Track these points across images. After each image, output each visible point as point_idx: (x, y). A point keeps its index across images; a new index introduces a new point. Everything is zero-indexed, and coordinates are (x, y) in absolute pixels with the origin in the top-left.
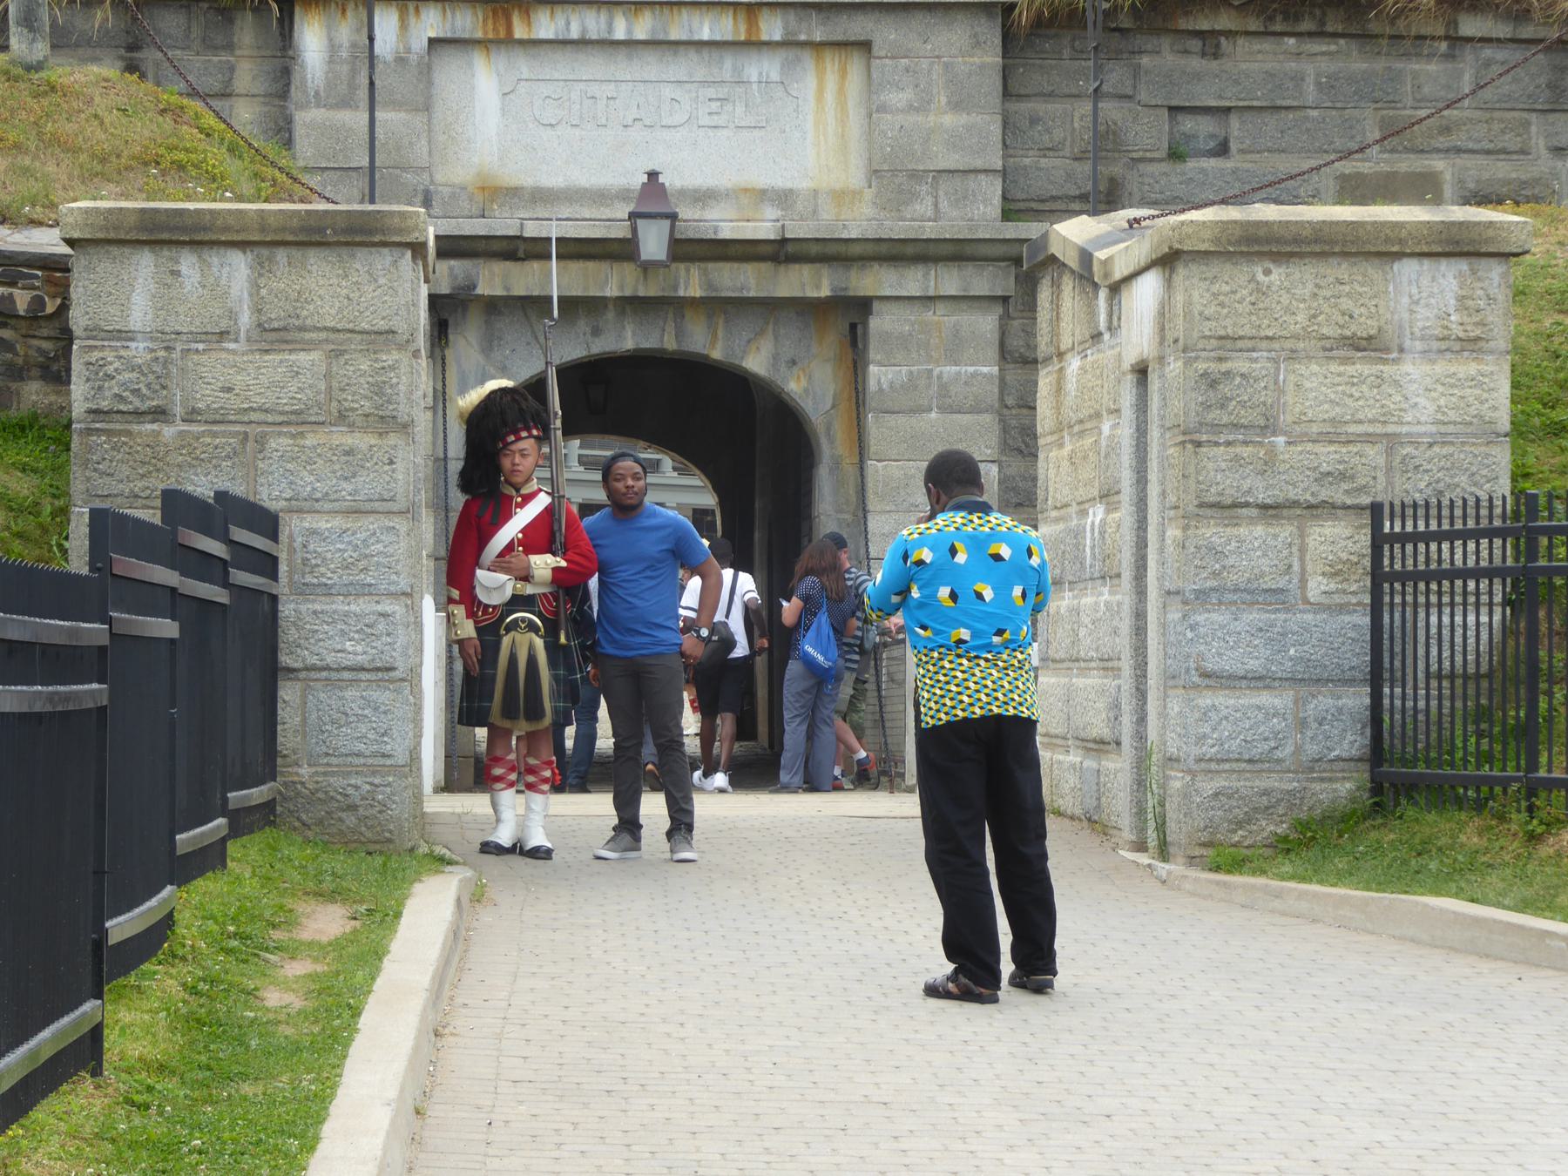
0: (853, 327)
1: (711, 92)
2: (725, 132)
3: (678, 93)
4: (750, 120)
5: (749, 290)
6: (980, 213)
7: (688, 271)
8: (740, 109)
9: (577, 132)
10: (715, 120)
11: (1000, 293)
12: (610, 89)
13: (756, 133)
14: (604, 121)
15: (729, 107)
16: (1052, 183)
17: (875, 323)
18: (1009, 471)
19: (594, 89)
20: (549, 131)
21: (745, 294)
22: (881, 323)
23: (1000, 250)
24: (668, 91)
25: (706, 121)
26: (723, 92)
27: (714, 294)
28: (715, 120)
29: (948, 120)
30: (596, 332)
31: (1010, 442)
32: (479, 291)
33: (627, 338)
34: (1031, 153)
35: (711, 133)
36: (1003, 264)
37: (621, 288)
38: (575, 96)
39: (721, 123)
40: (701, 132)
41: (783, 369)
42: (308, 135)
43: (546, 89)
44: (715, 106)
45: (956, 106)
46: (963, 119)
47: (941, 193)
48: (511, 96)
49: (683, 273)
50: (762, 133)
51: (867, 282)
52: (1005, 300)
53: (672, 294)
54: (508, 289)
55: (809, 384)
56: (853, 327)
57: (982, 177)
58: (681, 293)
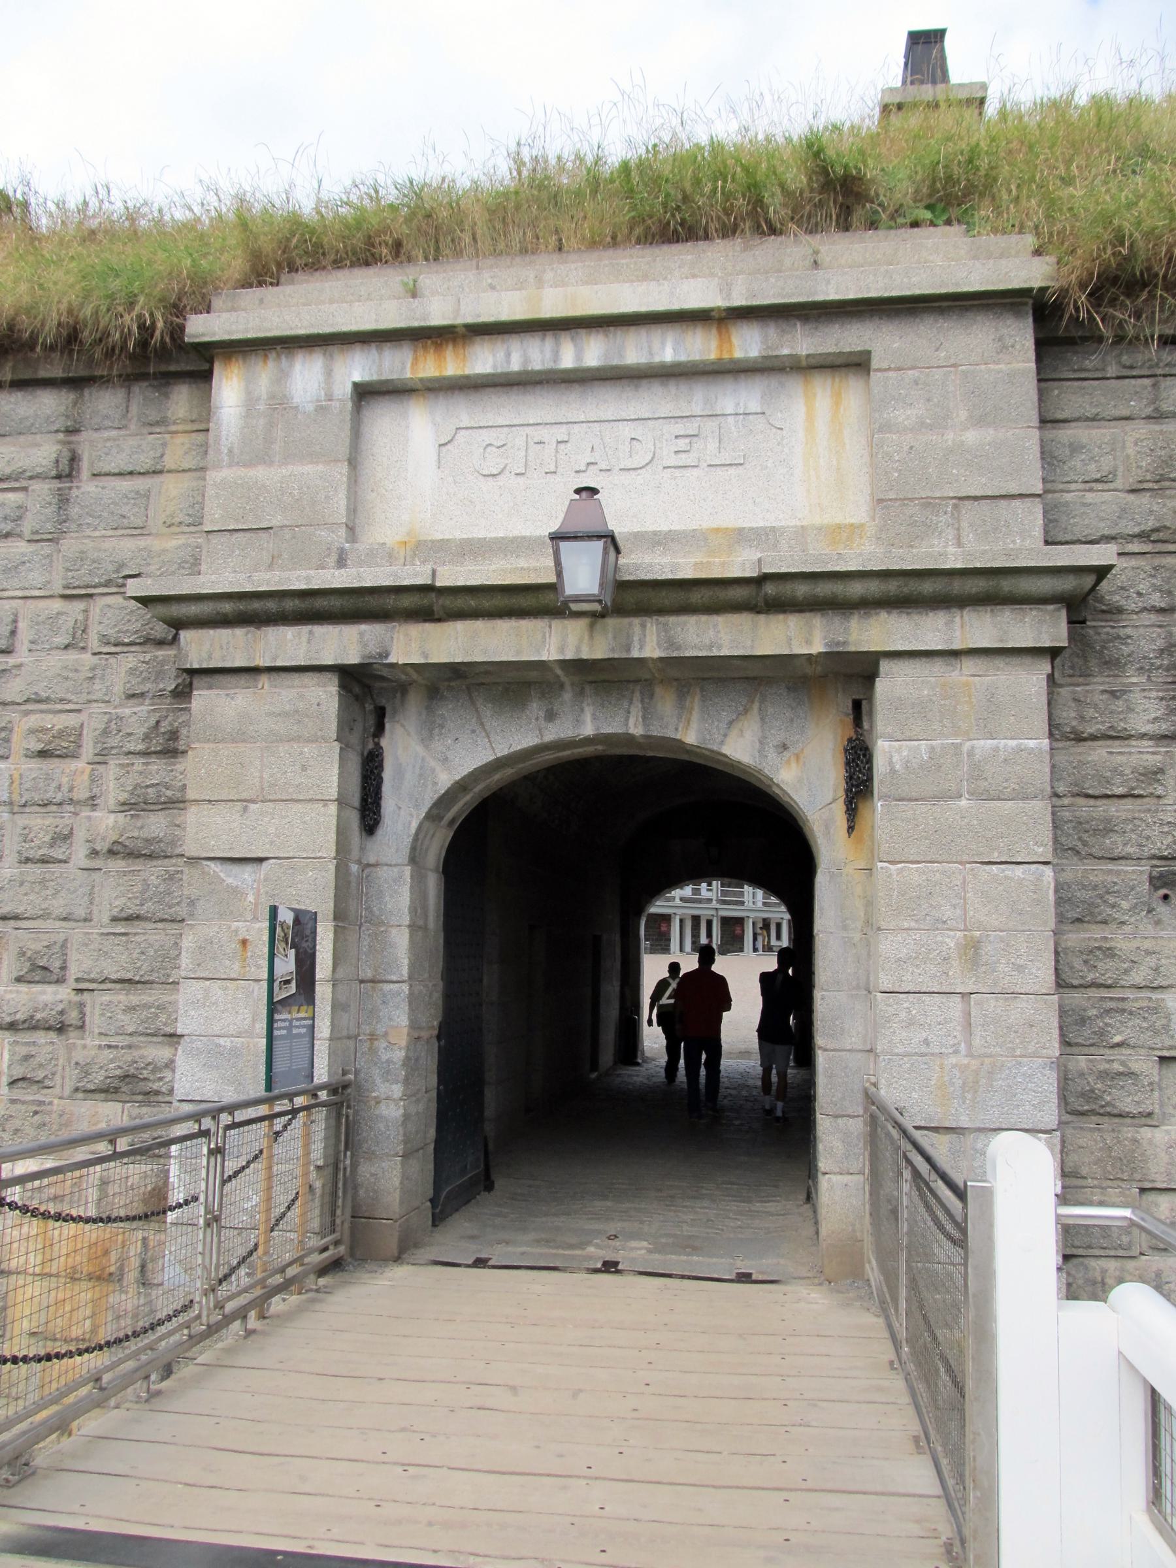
0: (857, 706)
1: (679, 428)
2: (695, 472)
3: (637, 430)
4: (725, 458)
5: (720, 647)
6: (1019, 541)
8: (712, 445)
9: (521, 480)
10: (683, 459)
12: (561, 433)
13: (732, 471)
14: (552, 469)
15: (698, 444)
16: (1102, 519)
17: (881, 686)
18: (1068, 876)
19: (543, 433)
21: (715, 653)
22: (891, 685)
23: (1046, 585)
24: (627, 430)
25: (673, 460)
26: (691, 427)
28: (683, 459)
29: (971, 437)
30: (551, 716)
31: (1063, 839)
32: (392, 659)
33: (585, 723)
34: (1073, 486)
35: (677, 473)
36: (1051, 607)
37: (562, 649)
38: (520, 441)
41: (772, 754)
42: (218, 496)
43: (486, 436)
44: (682, 444)
45: (980, 421)
46: (989, 434)
47: (964, 524)
48: (449, 447)
49: (637, 629)
52: (1053, 653)
53: (624, 655)
54: (426, 657)
55: (800, 768)
56: (857, 706)
57: (1017, 503)
58: (635, 654)
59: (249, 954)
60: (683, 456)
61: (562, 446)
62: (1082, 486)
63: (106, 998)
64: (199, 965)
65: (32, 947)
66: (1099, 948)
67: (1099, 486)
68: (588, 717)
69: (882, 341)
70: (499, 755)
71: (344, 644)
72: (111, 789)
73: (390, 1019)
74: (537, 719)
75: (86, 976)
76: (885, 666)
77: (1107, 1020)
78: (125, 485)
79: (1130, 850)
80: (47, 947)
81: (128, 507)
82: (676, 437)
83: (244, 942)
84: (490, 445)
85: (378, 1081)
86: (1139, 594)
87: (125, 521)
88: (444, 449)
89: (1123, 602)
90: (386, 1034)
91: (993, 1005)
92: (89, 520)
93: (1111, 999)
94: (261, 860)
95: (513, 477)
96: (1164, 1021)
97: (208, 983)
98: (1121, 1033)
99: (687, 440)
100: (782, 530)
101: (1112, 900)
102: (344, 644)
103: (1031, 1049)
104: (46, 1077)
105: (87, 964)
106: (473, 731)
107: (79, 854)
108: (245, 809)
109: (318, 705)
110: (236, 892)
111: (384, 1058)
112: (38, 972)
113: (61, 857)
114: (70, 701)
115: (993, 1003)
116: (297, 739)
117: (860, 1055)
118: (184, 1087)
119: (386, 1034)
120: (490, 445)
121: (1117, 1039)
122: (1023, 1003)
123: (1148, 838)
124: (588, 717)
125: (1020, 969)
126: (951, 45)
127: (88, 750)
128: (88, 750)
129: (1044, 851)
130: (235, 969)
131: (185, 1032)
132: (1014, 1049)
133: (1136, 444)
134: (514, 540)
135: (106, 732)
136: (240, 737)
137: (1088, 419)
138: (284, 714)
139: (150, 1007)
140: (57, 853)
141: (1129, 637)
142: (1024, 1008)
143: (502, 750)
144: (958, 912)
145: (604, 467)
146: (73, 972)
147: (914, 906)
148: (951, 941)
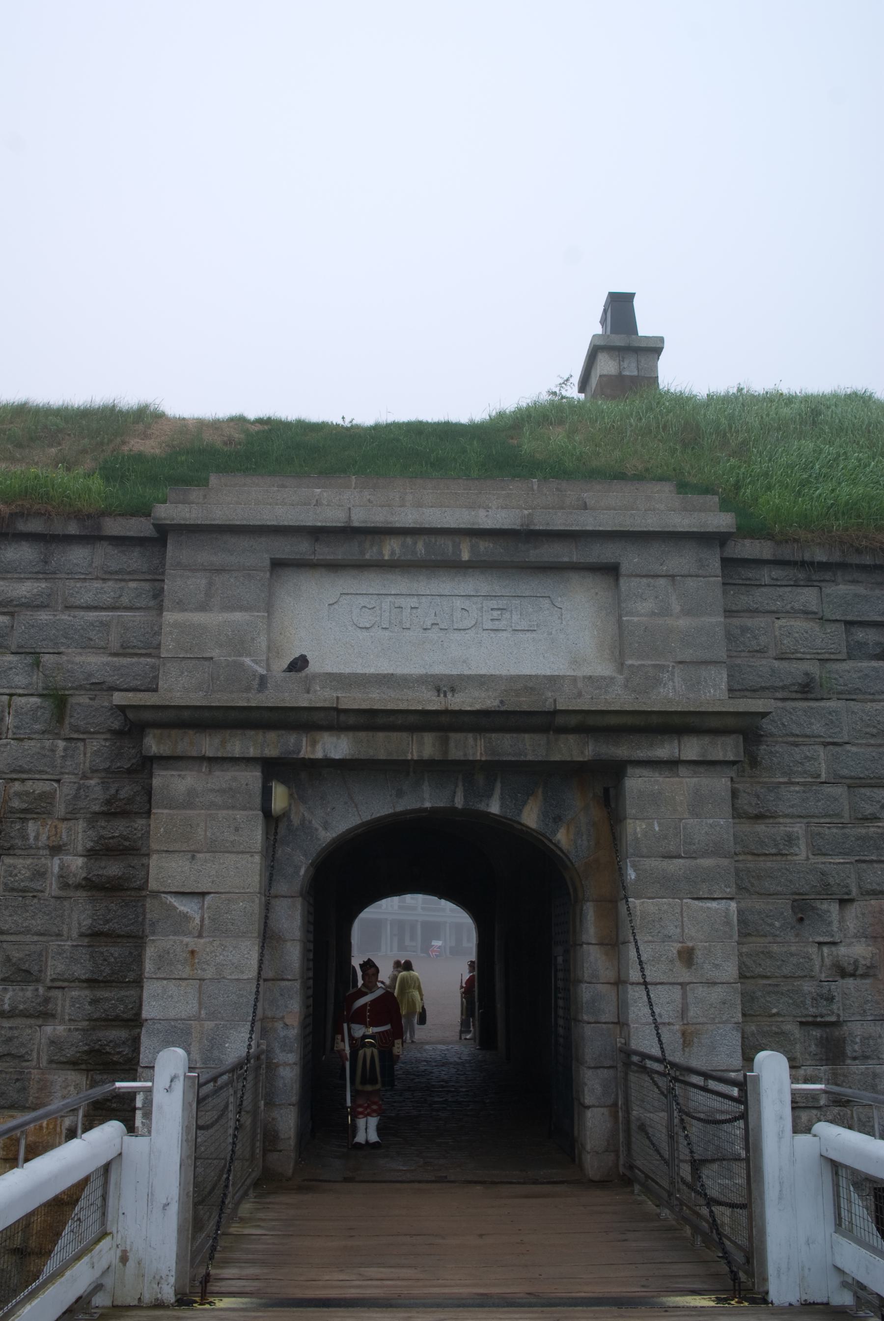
1: (493, 604)
2: (505, 634)
3: (467, 604)
4: (524, 625)
6: (713, 693)
7: (475, 740)
8: (515, 617)
11: (732, 758)
12: (413, 602)
13: (528, 634)
15: (507, 615)
16: (761, 677)
19: (401, 601)
20: (365, 633)
21: (522, 758)
22: (636, 783)
24: (458, 603)
25: (489, 625)
26: (502, 603)
27: (497, 758)
29: (683, 623)
30: (400, 794)
34: (743, 654)
35: (492, 634)
38: (386, 606)
39: (501, 627)
40: (485, 634)
43: (363, 601)
44: (496, 614)
45: (687, 612)
48: (336, 606)
50: (534, 635)
51: (621, 751)
56: (606, 791)
59: (197, 961)
60: (497, 623)
61: (414, 611)
62: (746, 654)
63: (75, 993)
64: (159, 969)
65: (17, 955)
66: (762, 952)
67: (759, 655)
68: (426, 796)
69: (631, 559)
70: (364, 820)
71: (271, 744)
72: (80, 839)
73: (286, 1007)
74: (391, 796)
75: (60, 977)
76: (630, 770)
77: (769, 999)
78: (92, 615)
79: (779, 889)
80: (29, 955)
81: (94, 633)
82: (492, 609)
83: (193, 952)
84: (365, 607)
85: (278, 1051)
86: (783, 724)
87: (92, 643)
88: (332, 608)
89: (773, 730)
90: (283, 1017)
91: (701, 991)
92: (64, 640)
93: (770, 985)
94: (203, 894)
95: (380, 630)
96: (802, 999)
97: (165, 982)
98: (776, 1007)
99: (499, 612)
100: (563, 677)
101: (769, 921)
102: (271, 744)
103: (724, 1018)
104: (27, 1052)
105: (61, 967)
106: (346, 803)
107: (53, 887)
108: (193, 857)
109: (247, 785)
110: (186, 917)
111: (282, 1034)
112: (23, 975)
113: (39, 888)
114: (47, 773)
115: (701, 989)
116: (233, 808)
117: (611, 1026)
118: (147, 1057)
119: (283, 1017)
120: (365, 607)
121: (774, 1011)
122: (719, 989)
123: (791, 881)
124: (426, 796)
125: (717, 966)
126: (637, 303)
127: (60, 809)
128: (60, 809)
129: (731, 890)
130: (187, 972)
131: (149, 1017)
132: (714, 1019)
133: (780, 629)
134: (385, 676)
135: (76, 797)
136: (188, 804)
137: (751, 611)
138: (222, 791)
139: (111, 1000)
140: (36, 885)
141: (777, 752)
142: (716, 994)
143: (367, 817)
144: (679, 930)
145: (443, 627)
146: (50, 973)
147: (651, 926)
148: (674, 948)
